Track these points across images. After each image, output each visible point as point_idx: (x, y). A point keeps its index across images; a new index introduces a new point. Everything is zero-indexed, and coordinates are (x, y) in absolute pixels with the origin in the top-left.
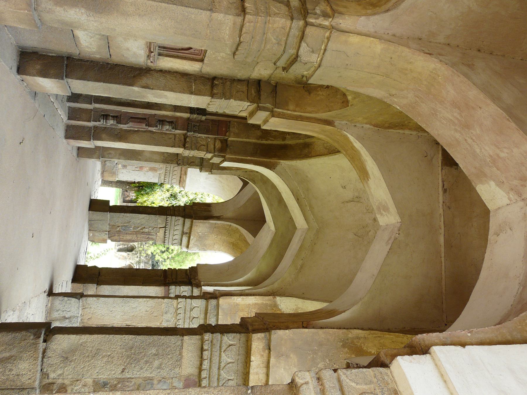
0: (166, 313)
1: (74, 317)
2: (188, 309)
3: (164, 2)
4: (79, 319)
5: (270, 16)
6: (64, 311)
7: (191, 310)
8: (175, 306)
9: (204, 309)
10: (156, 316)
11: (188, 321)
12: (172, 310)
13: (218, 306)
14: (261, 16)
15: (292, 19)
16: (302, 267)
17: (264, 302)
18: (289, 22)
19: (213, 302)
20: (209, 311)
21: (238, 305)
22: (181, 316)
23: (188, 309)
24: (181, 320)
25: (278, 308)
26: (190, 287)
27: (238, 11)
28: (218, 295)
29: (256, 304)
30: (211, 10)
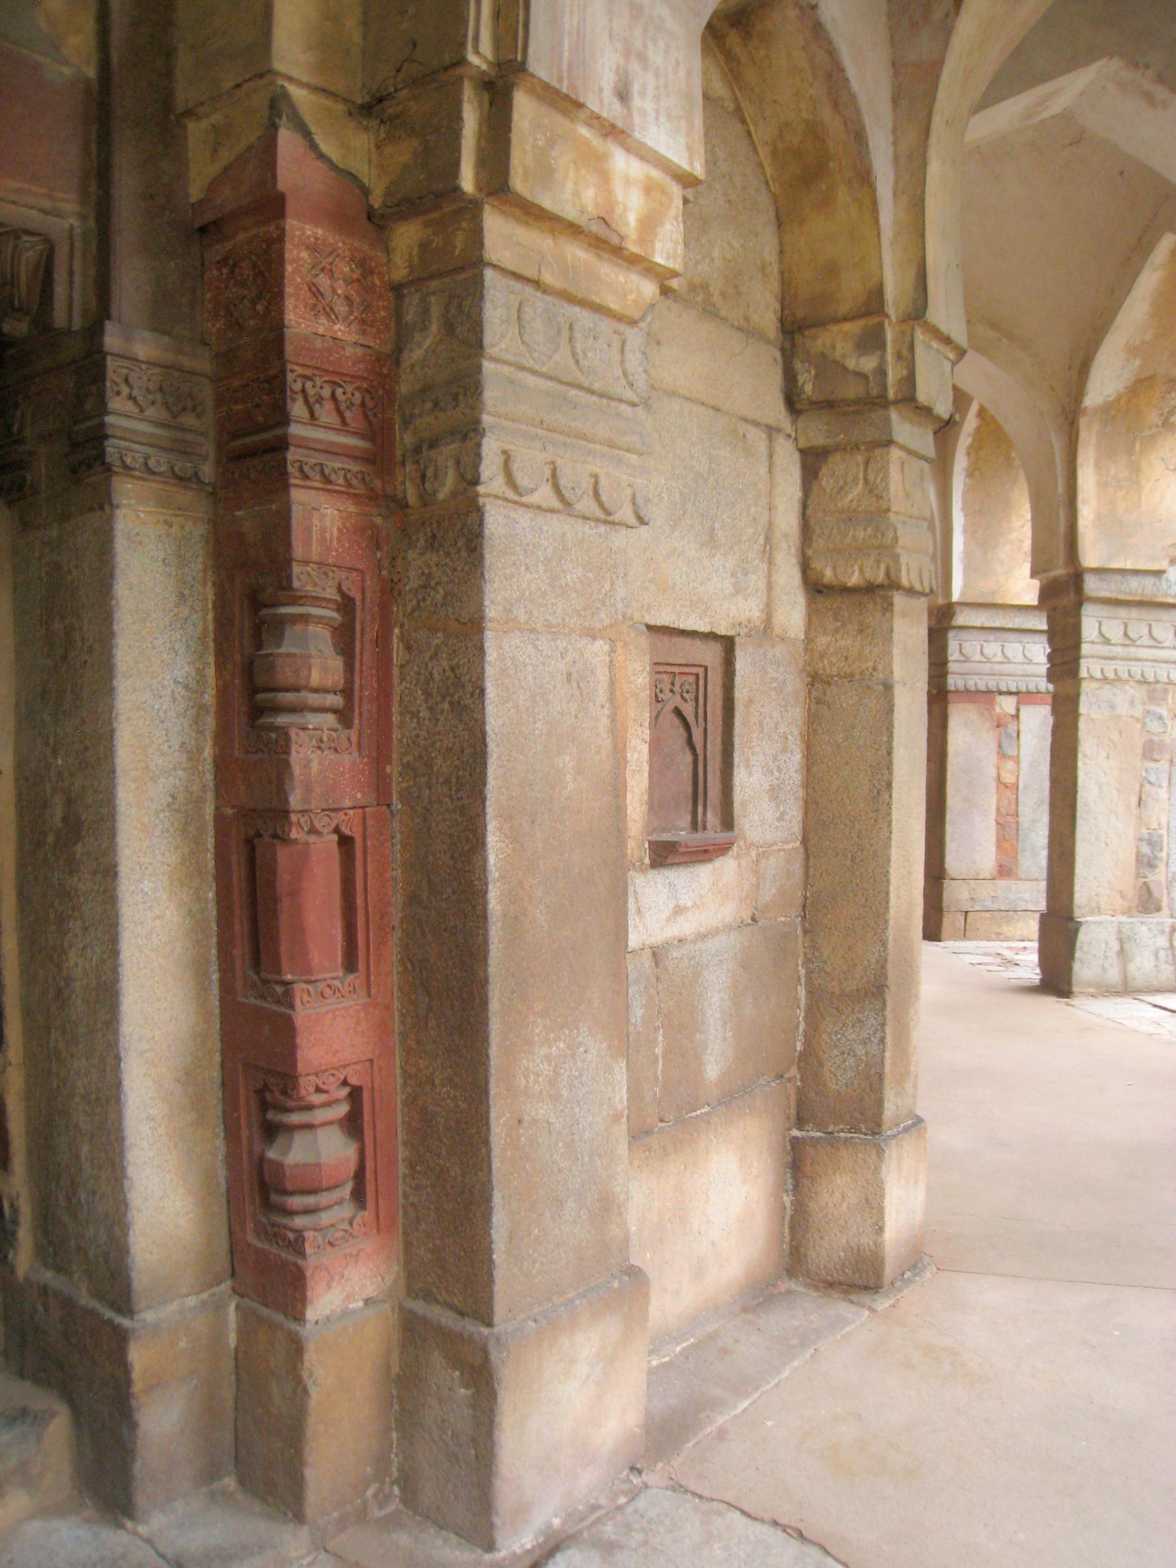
0: (1112, 707)
1: (1119, 931)
2: (1105, 650)
3: (889, 814)
4: (1123, 919)
5: (888, 510)
6: (1106, 957)
7: (1107, 642)
8: (1094, 685)
9: (1106, 608)
10: (1120, 733)
11: (1133, 649)
12: (1106, 692)
13: (1100, 571)
14: (896, 539)
15: (889, 443)
16: (994, 326)
17: (1094, 440)
18: (895, 454)
19: (1091, 585)
20: (1113, 595)
21: (1098, 516)
22: (1123, 668)
23: (1105, 650)
24: (1133, 669)
25: (1114, 401)
26: (951, 635)
27: (870, 606)
28: (1071, 570)
29: (1098, 465)
30: (888, 688)
